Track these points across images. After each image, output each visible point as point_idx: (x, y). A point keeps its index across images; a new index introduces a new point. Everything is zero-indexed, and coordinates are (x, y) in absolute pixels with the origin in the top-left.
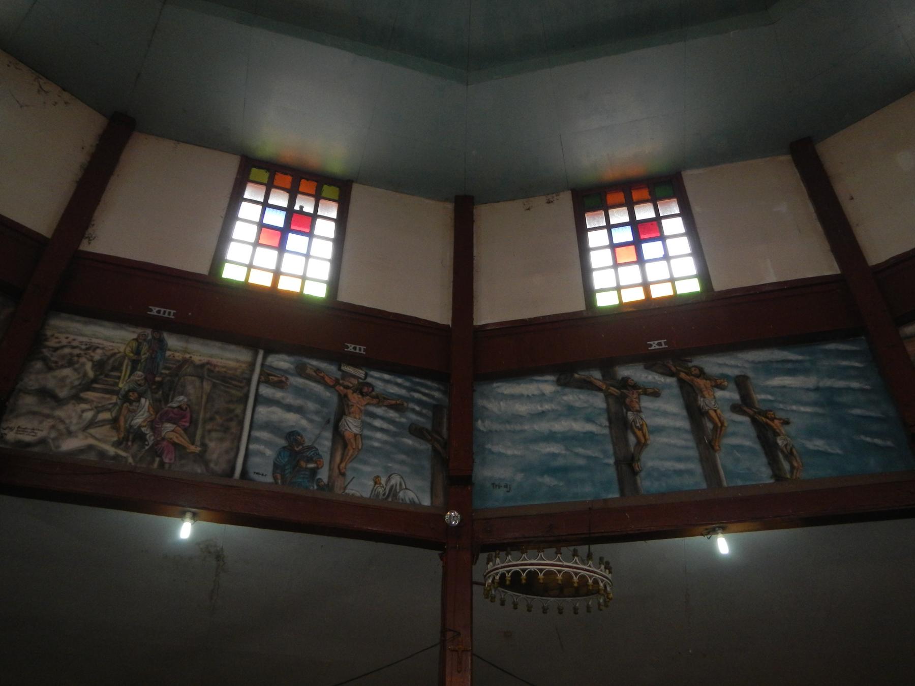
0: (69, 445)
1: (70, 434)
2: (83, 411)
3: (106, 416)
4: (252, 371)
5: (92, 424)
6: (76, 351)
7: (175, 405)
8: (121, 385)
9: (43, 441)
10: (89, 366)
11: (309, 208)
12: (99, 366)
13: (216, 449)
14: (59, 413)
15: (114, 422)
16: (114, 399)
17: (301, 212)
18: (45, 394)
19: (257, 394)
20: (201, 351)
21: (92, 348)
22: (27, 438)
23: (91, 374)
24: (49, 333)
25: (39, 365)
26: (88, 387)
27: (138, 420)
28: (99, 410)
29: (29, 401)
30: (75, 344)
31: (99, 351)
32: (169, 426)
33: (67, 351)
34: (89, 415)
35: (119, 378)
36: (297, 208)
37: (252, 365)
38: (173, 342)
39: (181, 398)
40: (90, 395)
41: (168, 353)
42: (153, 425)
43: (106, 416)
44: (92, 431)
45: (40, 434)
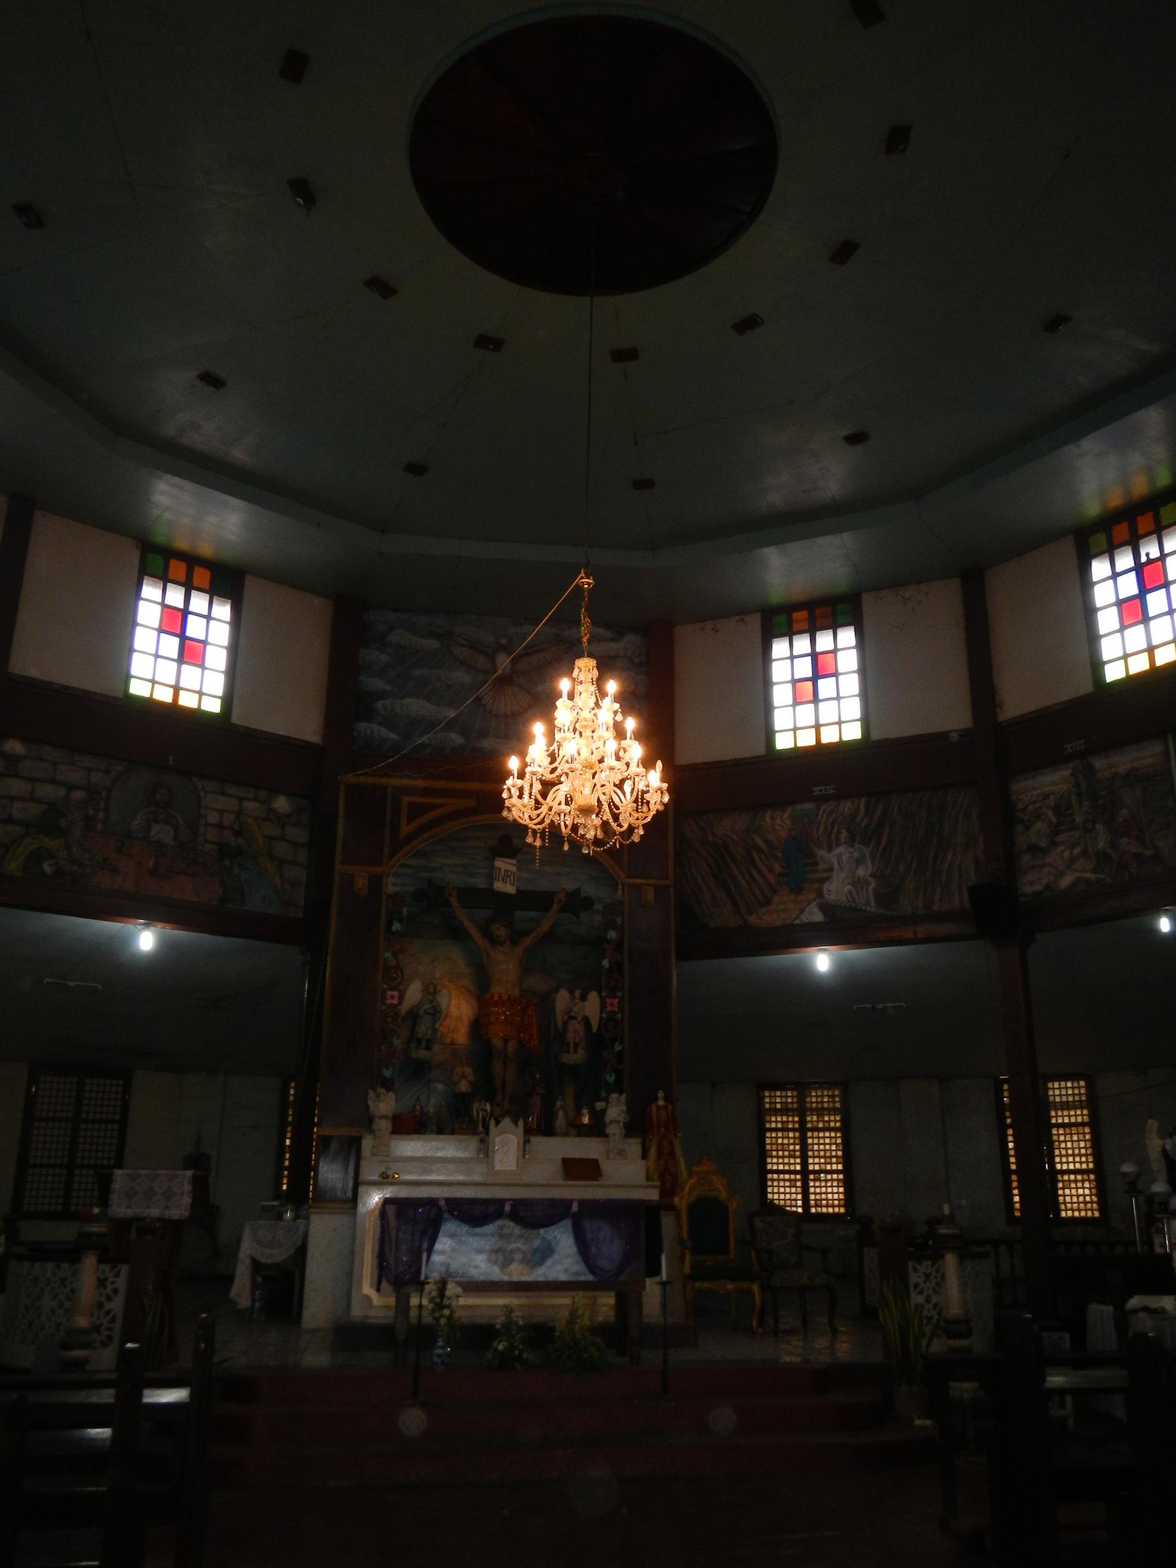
0: (1065, 882)
1: (1062, 874)
2: (1063, 852)
3: (1078, 850)
4: (1169, 760)
5: (1072, 860)
6: (1038, 805)
7: (1121, 820)
8: (1078, 820)
9: (1047, 887)
10: (1050, 813)
11: (1155, 553)
14: (1049, 860)
15: (1084, 853)
16: (1078, 834)
17: (1150, 562)
18: (1034, 849)
20: (1124, 761)
21: (1046, 796)
22: (1039, 888)
23: (1054, 820)
24: (1015, 798)
25: (1020, 828)
27: (1101, 844)
29: (1026, 859)
30: (1034, 798)
31: (1052, 797)
32: (1124, 840)
33: (1031, 807)
34: (1067, 854)
35: (1073, 814)
36: (1144, 559)
38: (1098, 763)
39: (1124, 811)
40: (1060, 838)
41: (1099, 775)
43: (1078, 850)
44: (1074, 866)
45: (1045, 881)
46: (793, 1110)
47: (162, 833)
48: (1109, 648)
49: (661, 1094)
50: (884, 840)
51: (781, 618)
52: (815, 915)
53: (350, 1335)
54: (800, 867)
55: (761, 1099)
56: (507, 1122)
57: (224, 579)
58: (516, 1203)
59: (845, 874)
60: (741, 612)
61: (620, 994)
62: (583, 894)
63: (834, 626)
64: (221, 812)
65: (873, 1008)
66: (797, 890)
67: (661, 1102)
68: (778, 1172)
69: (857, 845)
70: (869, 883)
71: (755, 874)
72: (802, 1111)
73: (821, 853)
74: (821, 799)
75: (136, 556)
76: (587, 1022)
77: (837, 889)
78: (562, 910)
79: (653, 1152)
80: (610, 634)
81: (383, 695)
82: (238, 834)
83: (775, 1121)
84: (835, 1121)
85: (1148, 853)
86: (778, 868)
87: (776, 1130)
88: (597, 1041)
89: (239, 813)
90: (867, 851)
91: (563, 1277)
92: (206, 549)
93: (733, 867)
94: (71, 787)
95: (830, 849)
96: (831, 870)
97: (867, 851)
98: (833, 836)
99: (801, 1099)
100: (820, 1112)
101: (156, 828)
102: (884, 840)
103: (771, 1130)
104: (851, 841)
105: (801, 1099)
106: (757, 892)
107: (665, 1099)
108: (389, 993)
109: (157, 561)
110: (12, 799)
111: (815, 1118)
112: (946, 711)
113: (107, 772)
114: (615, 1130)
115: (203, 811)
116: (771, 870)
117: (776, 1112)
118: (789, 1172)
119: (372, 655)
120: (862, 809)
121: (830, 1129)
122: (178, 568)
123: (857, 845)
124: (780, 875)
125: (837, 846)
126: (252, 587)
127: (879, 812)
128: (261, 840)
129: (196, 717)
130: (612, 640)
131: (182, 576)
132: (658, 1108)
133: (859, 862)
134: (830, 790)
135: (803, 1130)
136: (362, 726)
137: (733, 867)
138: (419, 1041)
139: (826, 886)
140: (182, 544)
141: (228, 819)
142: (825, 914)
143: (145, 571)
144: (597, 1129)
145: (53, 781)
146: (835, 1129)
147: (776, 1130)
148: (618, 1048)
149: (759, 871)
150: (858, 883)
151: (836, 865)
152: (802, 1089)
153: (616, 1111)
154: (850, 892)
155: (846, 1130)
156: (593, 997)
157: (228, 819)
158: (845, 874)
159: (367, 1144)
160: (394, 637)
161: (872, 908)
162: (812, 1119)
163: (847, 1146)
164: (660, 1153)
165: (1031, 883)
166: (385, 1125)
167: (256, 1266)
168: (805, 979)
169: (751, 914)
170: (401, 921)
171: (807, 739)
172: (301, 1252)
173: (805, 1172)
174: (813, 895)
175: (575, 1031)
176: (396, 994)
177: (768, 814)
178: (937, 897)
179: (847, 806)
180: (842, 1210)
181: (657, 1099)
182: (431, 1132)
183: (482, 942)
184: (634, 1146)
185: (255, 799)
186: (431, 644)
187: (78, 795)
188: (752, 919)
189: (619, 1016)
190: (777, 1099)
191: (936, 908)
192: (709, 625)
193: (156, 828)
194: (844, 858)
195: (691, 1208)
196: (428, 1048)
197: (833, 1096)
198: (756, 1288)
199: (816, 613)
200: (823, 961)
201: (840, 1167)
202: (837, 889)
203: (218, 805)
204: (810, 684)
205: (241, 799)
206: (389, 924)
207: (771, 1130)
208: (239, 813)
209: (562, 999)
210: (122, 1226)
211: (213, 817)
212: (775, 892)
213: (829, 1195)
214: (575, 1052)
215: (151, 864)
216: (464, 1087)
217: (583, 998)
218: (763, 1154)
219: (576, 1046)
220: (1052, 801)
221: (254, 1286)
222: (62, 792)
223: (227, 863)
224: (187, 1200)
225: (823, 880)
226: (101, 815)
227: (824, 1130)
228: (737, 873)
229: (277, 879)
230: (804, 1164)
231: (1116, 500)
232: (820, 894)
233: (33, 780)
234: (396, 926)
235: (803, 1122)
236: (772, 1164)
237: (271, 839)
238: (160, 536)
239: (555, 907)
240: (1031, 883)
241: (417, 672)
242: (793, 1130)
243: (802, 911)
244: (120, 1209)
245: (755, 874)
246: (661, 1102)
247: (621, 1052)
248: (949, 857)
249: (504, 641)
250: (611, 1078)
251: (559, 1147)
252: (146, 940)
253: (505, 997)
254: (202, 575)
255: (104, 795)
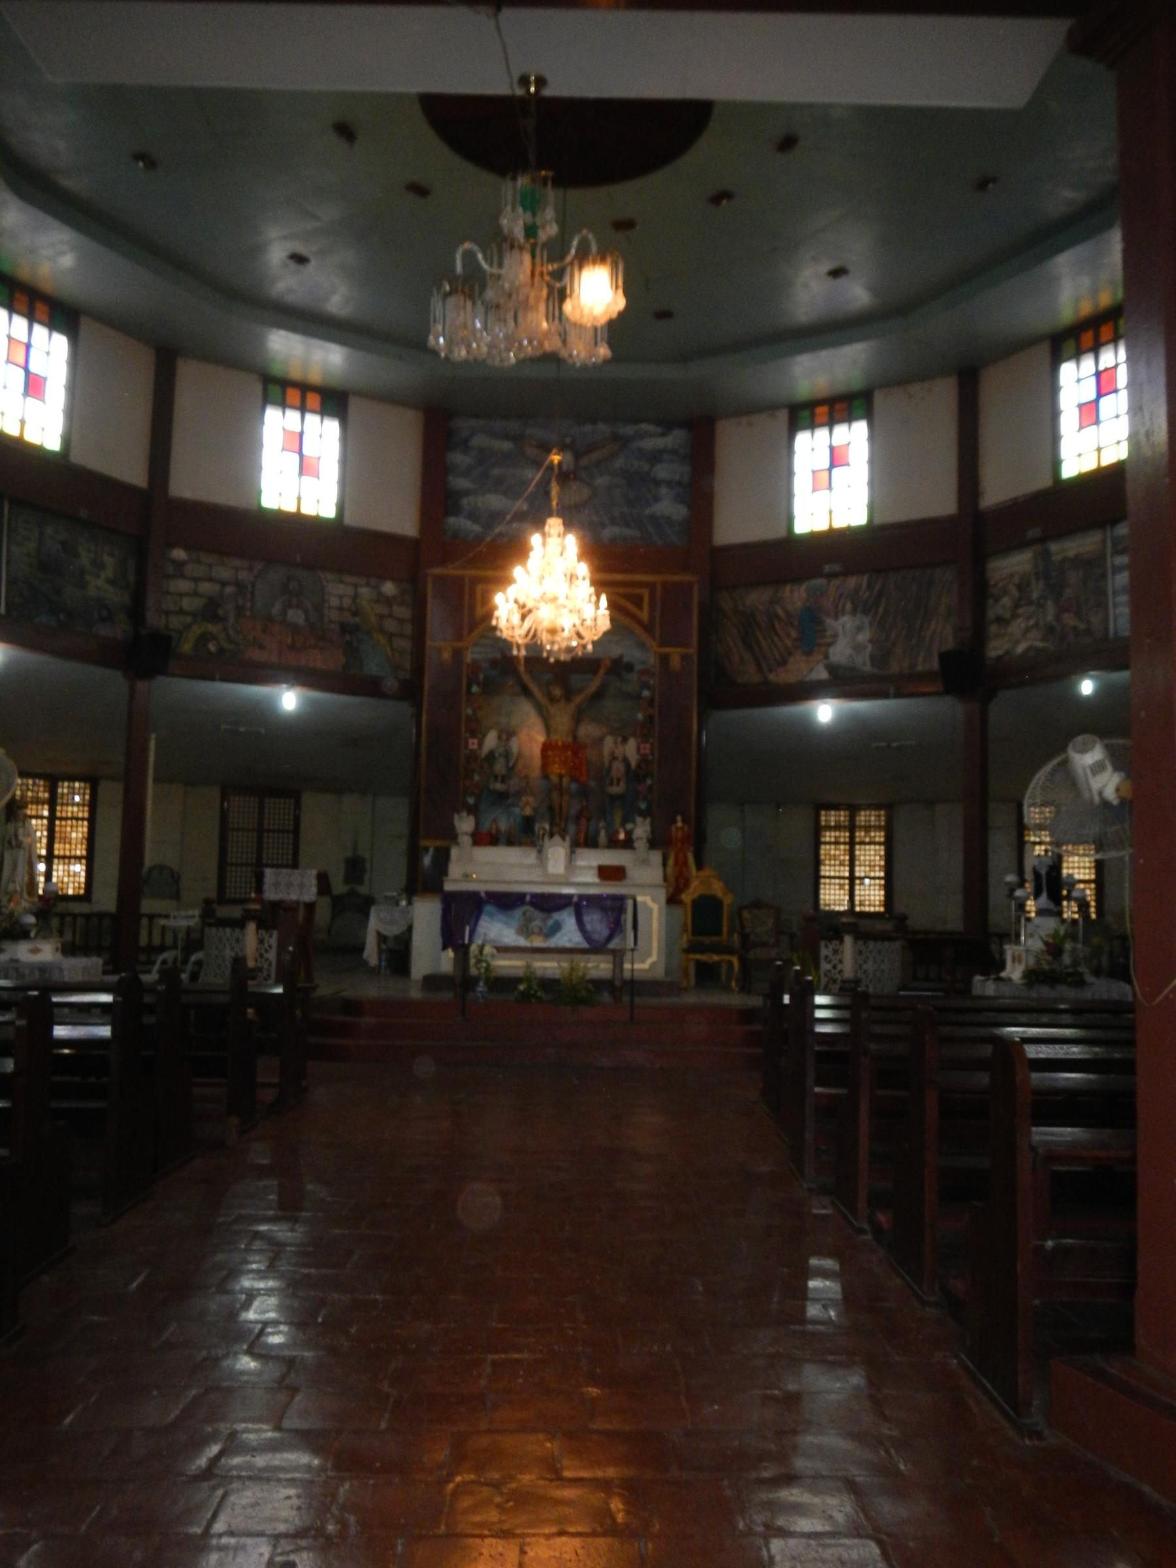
0: (1020, 648)
1: (1017, 642)
3: (1032, 622)
9: (1007, 653)
12: (1019, 587)
13: (1095, 620)
14: (1010, 629)
15: (1036, 625)
16: (1033, 608)
18: (1000, 620)
19: (1113, 566)
21: (1012, 575)
22: (1000, 652)
25: (991, 601)
26: (1017, 605)
28: (1029, 618)
29: (993, 629)
34: (1023, 625)
37: (1104, 541)
38: (1054, 547)
40: (1021, 611)
42: (1058, 617)
46: (845, 827)
47: (296, 616)
48: (1067, 450)
49: (679, 818)
50: (881, 610)
51: (805, 414)
52: (822, 674)
53: (432, 981)
54: (811, 632)
55: (818, 817)
56: (557, 838)
57: (332, 400)
58: (535, 896)
59: (849, 638)
60: (771, 408)
61: (651, 740)
62: (625, 660)
63: (849, 419)
64: (341, 597)
65: (889, 747)
66: (808, 653)
67: (679, 824)
68: (829, 877)
69: (858, 615)
70: (865, 647)
71: (776, 639)
72: (852, 828)
73: (829, 621)
74: (831, 576)
75: (258, 389)
76: (626, 761)
77: (840, 652)
78: (607, 673)
79: (671, 862)
80: (659, 430)
81: (467, 493)
82: (355, 614)
83: (828, 836)
84: (880, 836)
85: (1082, 626)
86: (794, 634)
87: (830, 843)
88: (635, 775)
89: (355, 597)
90: (866, 620)
91: (568, 945)
92: (315, 376)
93: (759, 634)
94: (224, 584)
95: (836, 618)
96: (835, 636)
97: (866, 620)
98: (840, 607)
99: (852, 818)
100: (867, 828)
101: (291, 613)
102: (881, 610)
103: (826, 843)
104: (854, 611)
105: (852, 818)
106: (775, 652)
107: (684, 821)
108: (471, 741)
109: (275, 390)
110: (181, 595)
111: (863, 834)
112: (940, 501)
113: (250, 569)
114: (641, 845)
115: (326, 597)
116: (788, 635)
117: (829, 828)
118: (839, 878)
119: (458, 458)
120: (865, 583)
121: (875, 843)
122: (293, 395)
123: (858, 615)
124: (796, 640)
125: (843, 614)
126: (354, 404)
127: (877, 587)
128: (373, 619)
129: (316, 523)
130: (663, 435)
131: (297, 402)
132: (677, 828)
133: (859, 629)
134: (837, 568)
135: (852, 843)
136: (452, 520)
137: (759, 634)
138: (496, 777)
139: (831, 650)
140: (295, 374)
141: (347, 602)
142: (830, 673)
143: (267, 400)
144: (628, 844)
145: (210, 579)
146: (879, 844)
147: (830, 843)
148: (649, 782)
149: (779, 637)
150: (858, 648)
151: (840, 632)
152: (853, 810)
153: (642, 830)
154: (851, 656)
155: (889, 844)
156: (632, 744)
157: (347, 602)
158: (849, 638)
159: (454, 852)
160: (478, 441)
161: (868, 668)
162: (860, 835)
163: (889, 858)
164: (676, 863)
165: (995, 649)
166: (466, 840)
167: (382, 938)
168: (807, 727)
169: (770, 671)
170: (478, 684)
171: (821, 526)
172: (410, 929)
173: (852, 878)
174: (821, 657)
175: (618, 768)
176: (476, 741)
177: (788, 588)
178: (920, 659)
179: (852, 582)
180: (882, 909)
181: (675, 822)
182: (503, 844)
183: (544, 701)
184: (656, 857)
185: (368, 585)
186: (506, 446)
187: (229, 590)
188: (772, 677)
189: (650, 757)
190: (831, 817)
191: (920, 668)
192: (744, 420)
193: (291, 613)
194: (848, 626)
195: (694, 901)
196: (503, 781)
197: (879, 816)
198: (735, 960)
199: (837, 407)
200: (825, 712)
201: (882, 874)
202: (840, 652)
203: (338, 592)
204: (826, 474)
205: (356, 586)
206: (469, 687)
207: (826, 843)
208: (355, 597)
209: (609, 742)
210: (276, 906)
211: (334, 602)
212: (790, 654)
213: (871, 896)
214: (618, 784)
215: (289, 641)
216: (528, 811)
217: (625, 740)
218: (817, 863)
219: (619, 780)
220: (1016, 580)
221: (380, 951)
222: (217, 587)
223: (348, 638)
224: (314, 890)
225: (830, 645)
226: (249, 604)
227: (870, 843)
228: (761, 638)
229: (389, 650)
230: (852, 871)
231: (1086, 309)
232: (826, 656)
233: (196, 580)
234: (475, 689)
235: (852, 837)
236: (825, 870)
237: (381, 617)
238: (277, 369)
239: (602, 672)
240: (995, 649)
241: (496, 472)
242: (844, 843)
243: (811, 670)
244: (270, 894)
245: (776, 639)
246: (679, 824)
247: (650, 787)
248: (933, 627)
249: (568, 440)
250: (643, 806)
251: (591, 859)
252: (289, 700)
253: (560, 743)
254: (314, 400)
255: (250, 589)
